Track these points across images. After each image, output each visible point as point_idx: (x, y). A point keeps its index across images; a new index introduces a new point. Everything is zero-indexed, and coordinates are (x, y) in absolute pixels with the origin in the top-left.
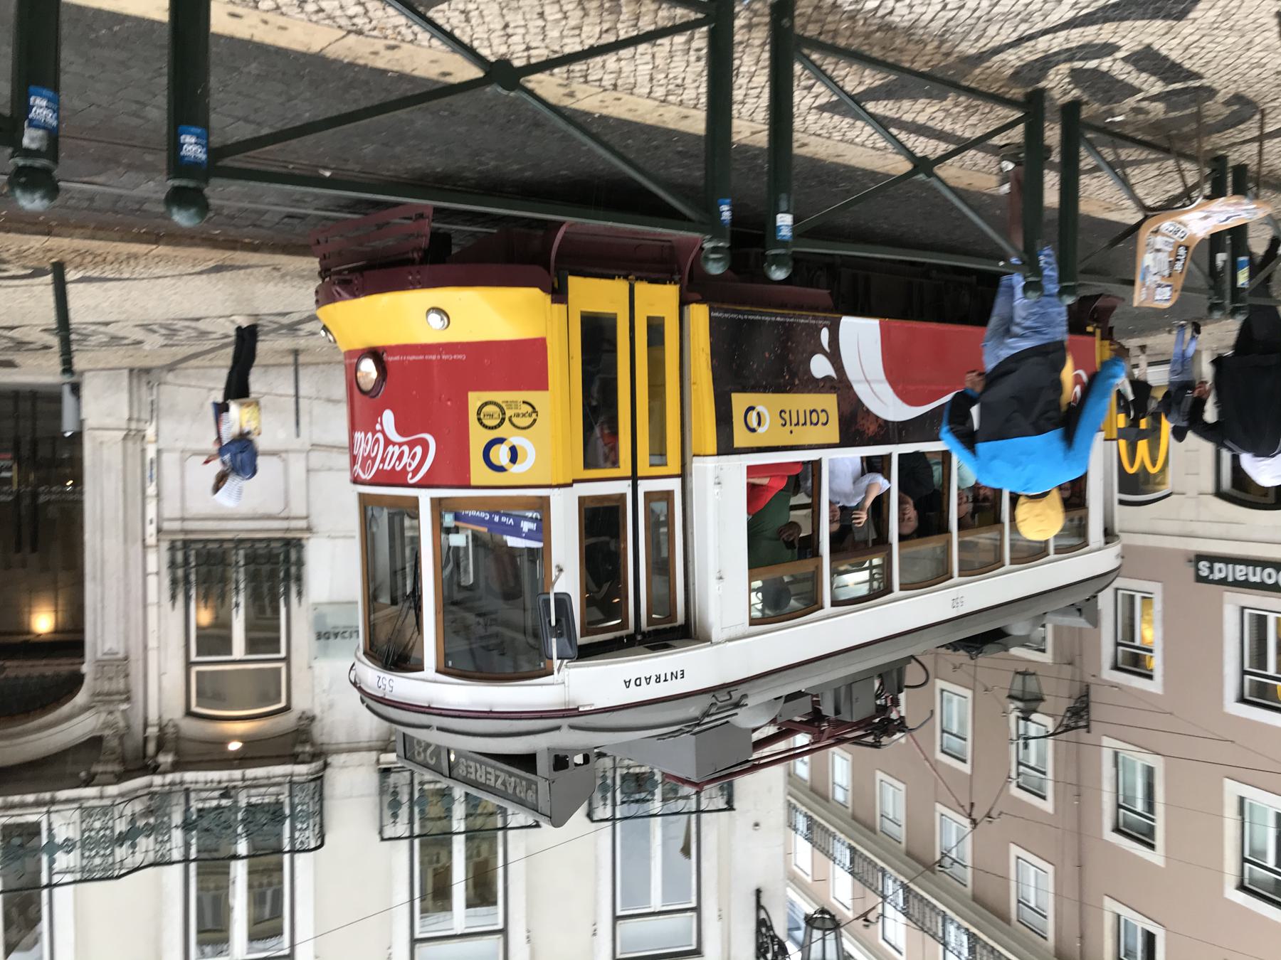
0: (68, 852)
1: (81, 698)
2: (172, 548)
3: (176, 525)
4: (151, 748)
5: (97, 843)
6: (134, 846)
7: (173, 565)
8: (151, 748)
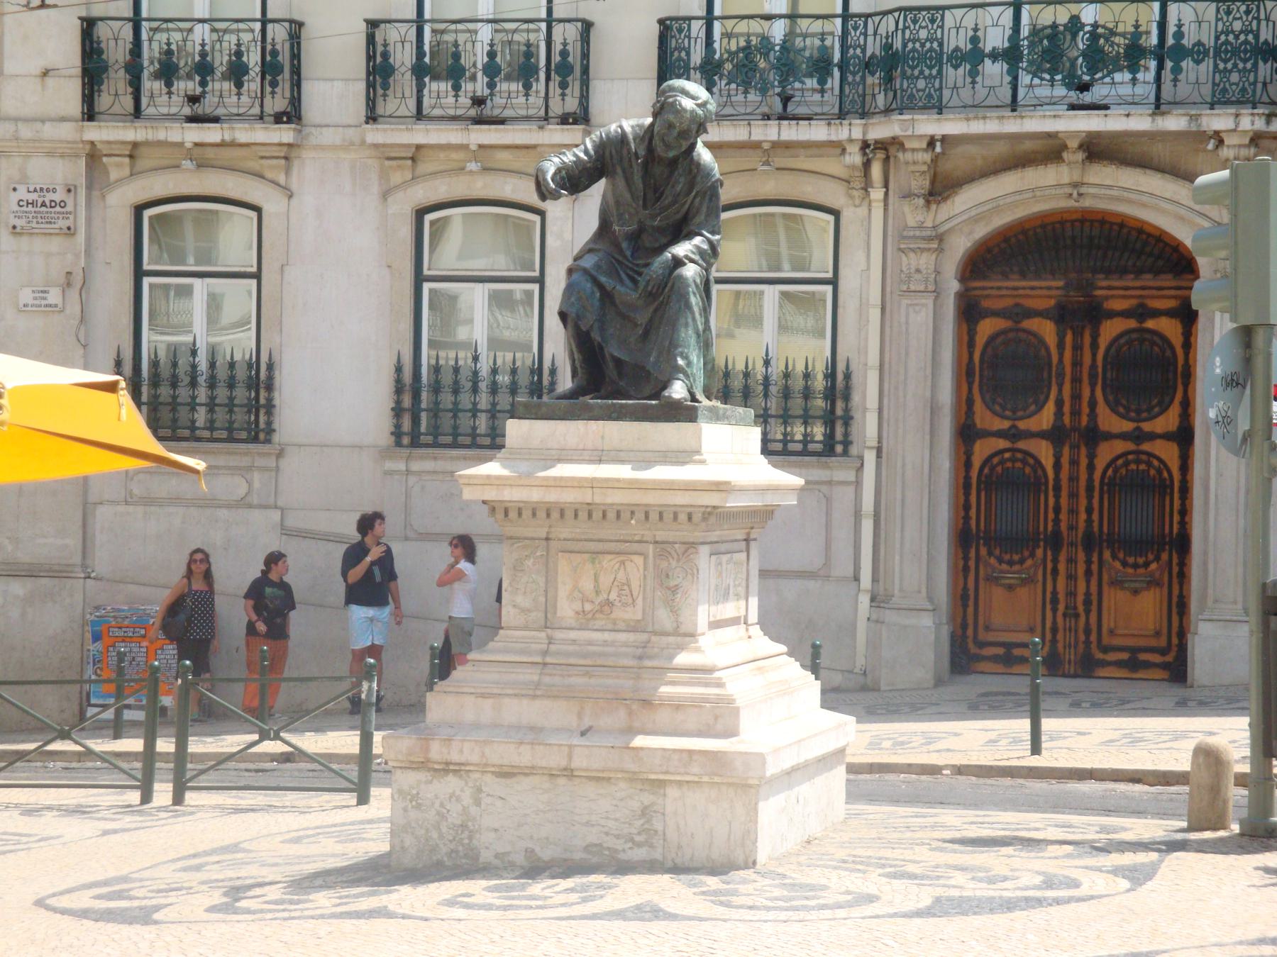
0: (957, 49)
1: (961, 245)
2: (847, 443)
3: (840, 475)
4: (876, 170)
5: (922, 58)
6: (888, 47)
7: (847, 420)
8: (876, 170)
